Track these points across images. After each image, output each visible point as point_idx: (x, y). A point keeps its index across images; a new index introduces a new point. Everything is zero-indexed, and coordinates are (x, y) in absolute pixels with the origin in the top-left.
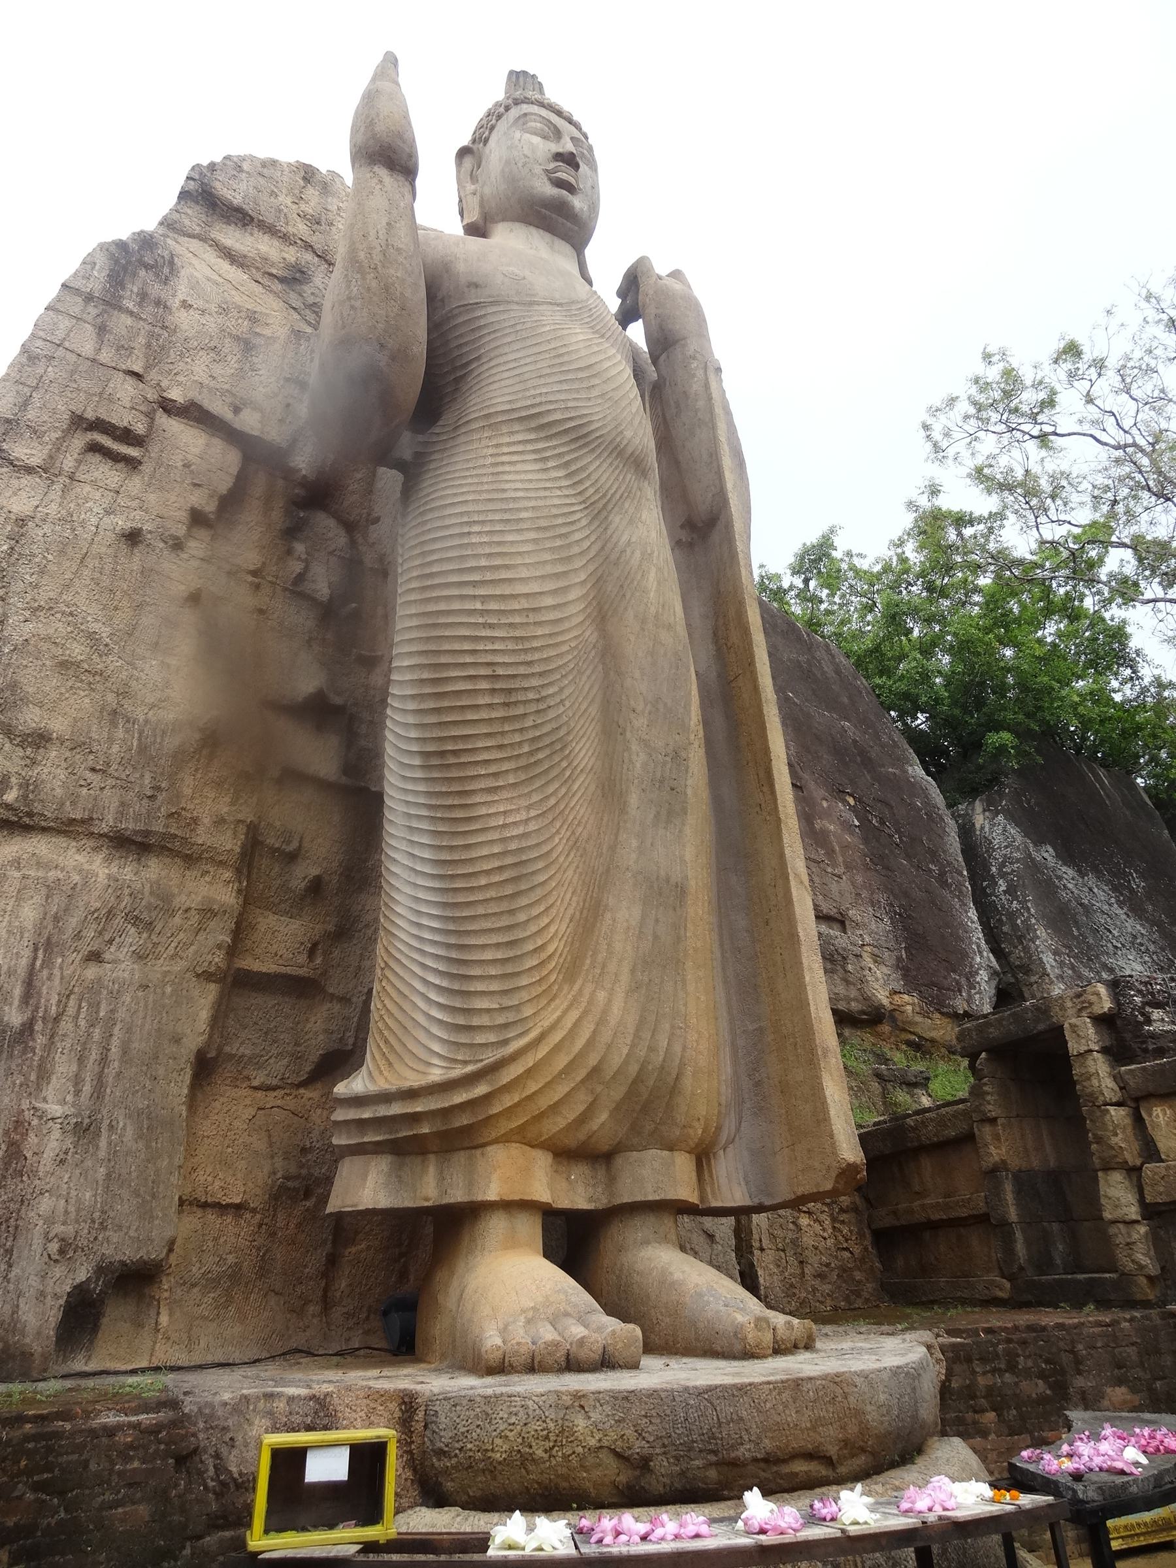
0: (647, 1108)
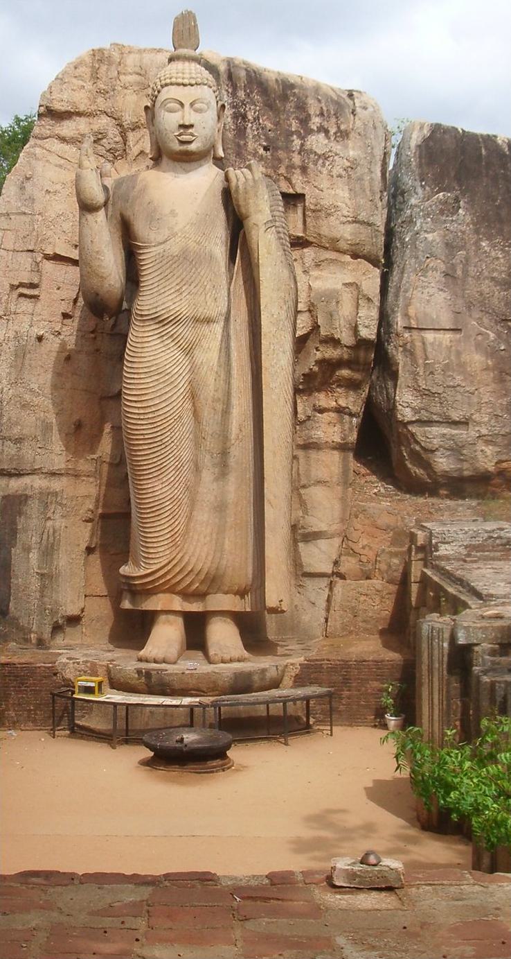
0: (213, 582)
